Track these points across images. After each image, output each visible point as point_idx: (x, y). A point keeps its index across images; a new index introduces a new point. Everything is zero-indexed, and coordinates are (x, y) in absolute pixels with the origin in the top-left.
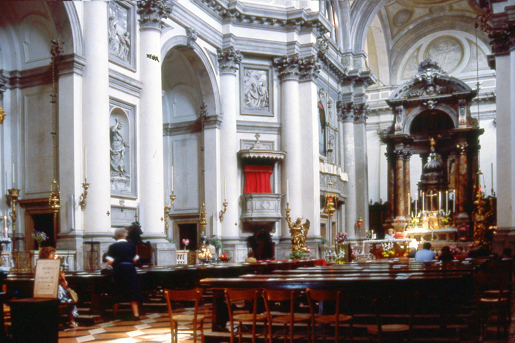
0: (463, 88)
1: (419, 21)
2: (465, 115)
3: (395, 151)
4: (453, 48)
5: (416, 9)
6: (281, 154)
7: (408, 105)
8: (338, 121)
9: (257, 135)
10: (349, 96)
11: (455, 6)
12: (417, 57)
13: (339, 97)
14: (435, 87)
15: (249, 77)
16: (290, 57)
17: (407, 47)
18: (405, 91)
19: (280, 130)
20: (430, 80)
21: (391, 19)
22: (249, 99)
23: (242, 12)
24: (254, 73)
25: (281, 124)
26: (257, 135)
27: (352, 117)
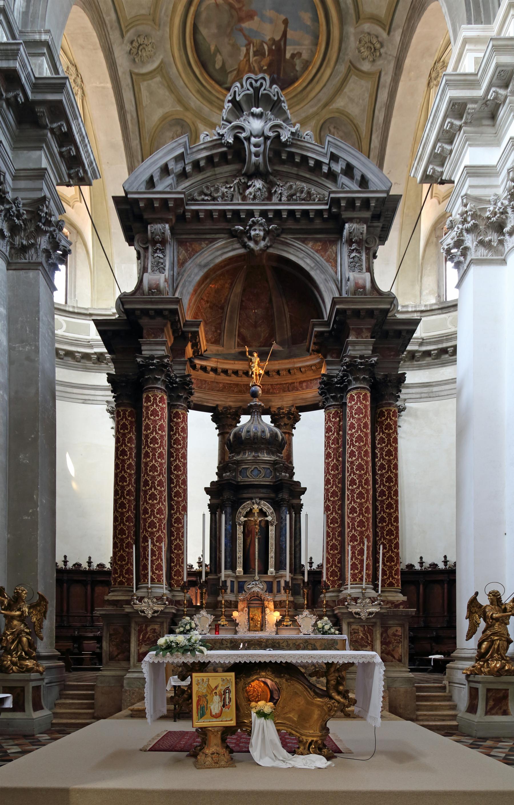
20: (255, 153)
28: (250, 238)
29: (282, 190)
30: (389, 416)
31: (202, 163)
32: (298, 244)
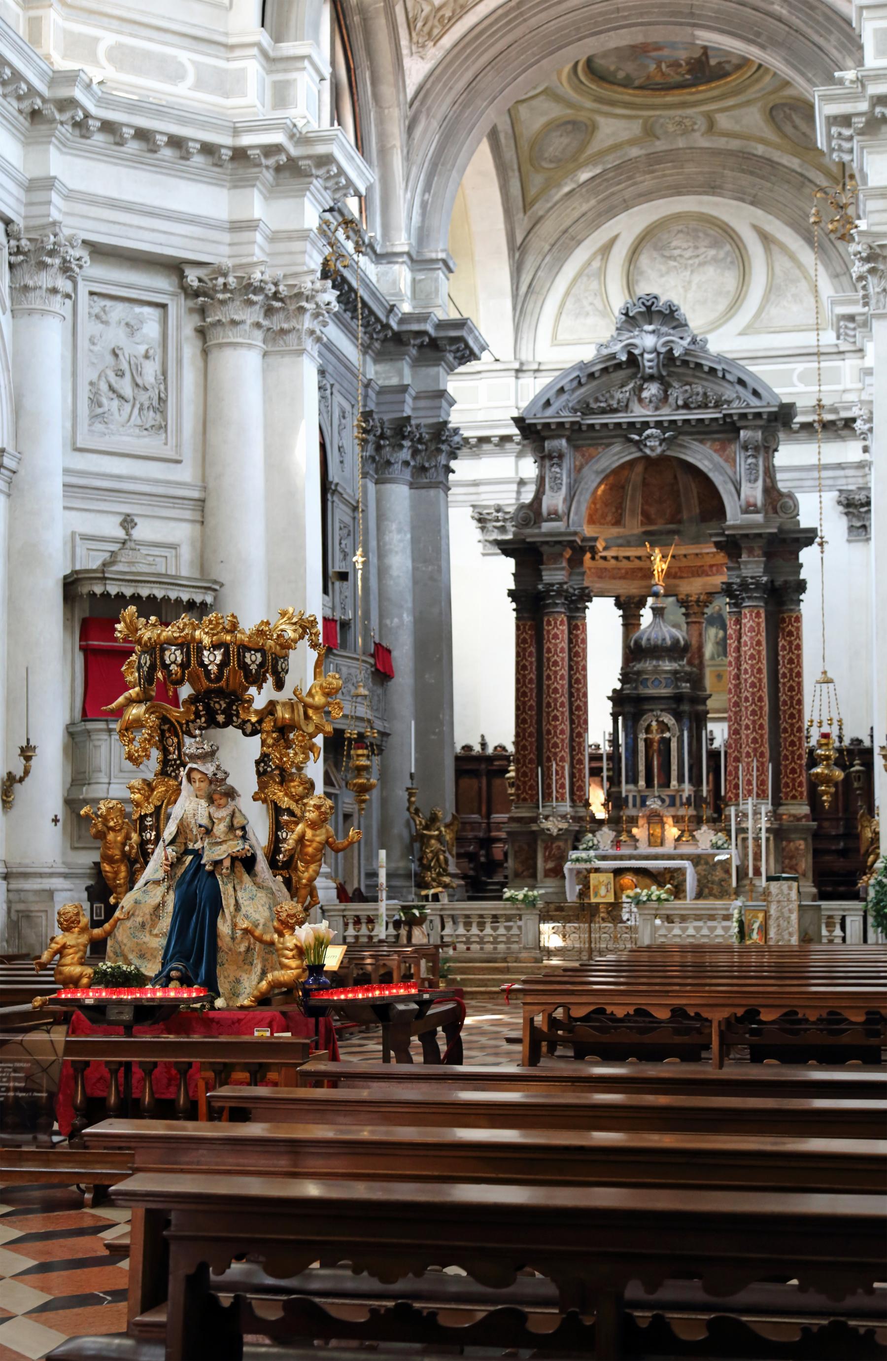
0: (755, 393)
1: (611, 161)
2: (760, 483)
3: (540, 587)
4: (712, 252)
5: (601, 120)
6: (209, 588)
7: (582, 436)
8: (365, 475)
9: (128, 522)
10: (398, 397)
11: (723, 121)
13: (366, 396)
14: (666, 386)
15: (106, 323)
16: (237, 267)
18: (574, 390)
19: (202, 508)
21: (525, 146)
22: (104, 401)
23: (93, 110)
24: (118, 311)
25: (205, 489)
26: (128, 522)
28: (645, 445)
29: (677, 393)
30: (790, 623)
31: (597, 375)
32: (696, 445)
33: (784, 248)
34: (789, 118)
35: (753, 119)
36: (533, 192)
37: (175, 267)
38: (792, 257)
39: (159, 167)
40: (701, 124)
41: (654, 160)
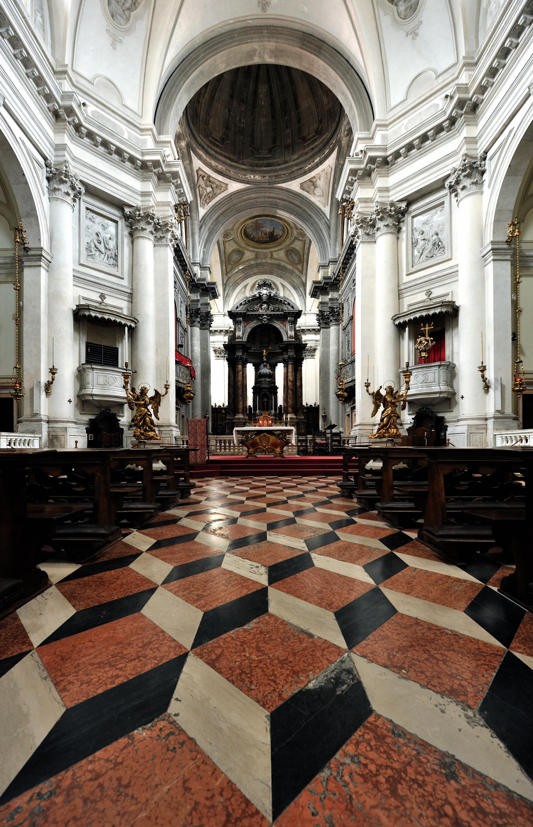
0: (293, 307)
1: (247, 264)
5: (246, 251)
9: (102, 296)
11: (275, 255)
12: (244, 292)
15: (94, 222)
17: (236, 284)
19: (131, 297)
21: (227, 256)
22: (93, 250)
24: (98, 219)
25: (132, 289)
27: (199, 322)
33: (287, 288)
34: (291, 254)
35: (282, 254)
36: (228, 270)
37: (119, 205)
38: (289, 291)
39: (112, 161)
40: (269, 256)
41: (257, 265)
